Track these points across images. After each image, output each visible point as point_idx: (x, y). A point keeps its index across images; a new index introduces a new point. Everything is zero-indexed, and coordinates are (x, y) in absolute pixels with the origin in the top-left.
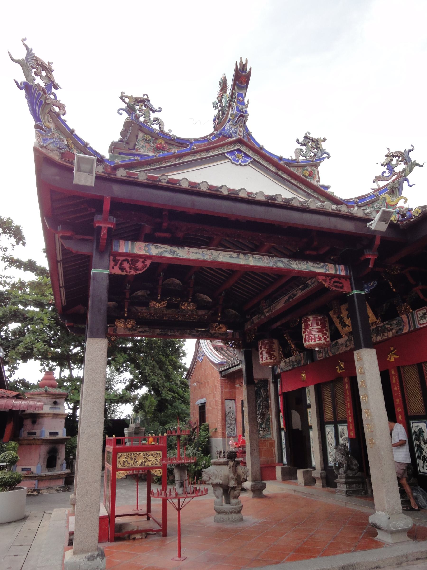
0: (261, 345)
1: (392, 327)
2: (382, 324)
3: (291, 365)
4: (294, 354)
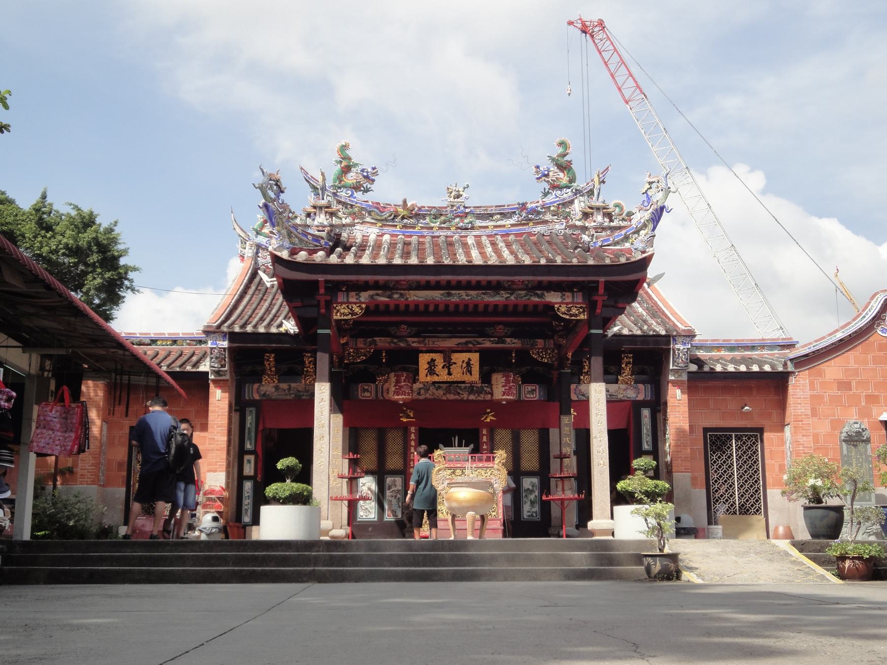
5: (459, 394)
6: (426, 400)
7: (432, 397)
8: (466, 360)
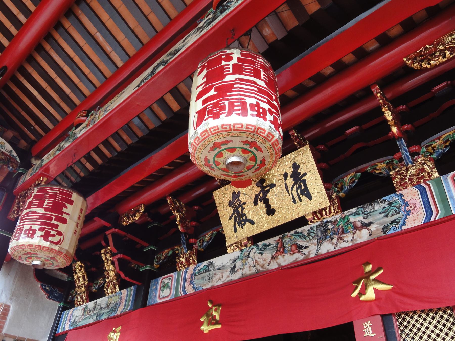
0: (31, 199)
1: (370, 219)
2: (339, 216)
3: (95, 314)
4: (110, 290)
5: (300, 247)
6: (244, 279)
7: (254, 271)
8: (290, 171)
